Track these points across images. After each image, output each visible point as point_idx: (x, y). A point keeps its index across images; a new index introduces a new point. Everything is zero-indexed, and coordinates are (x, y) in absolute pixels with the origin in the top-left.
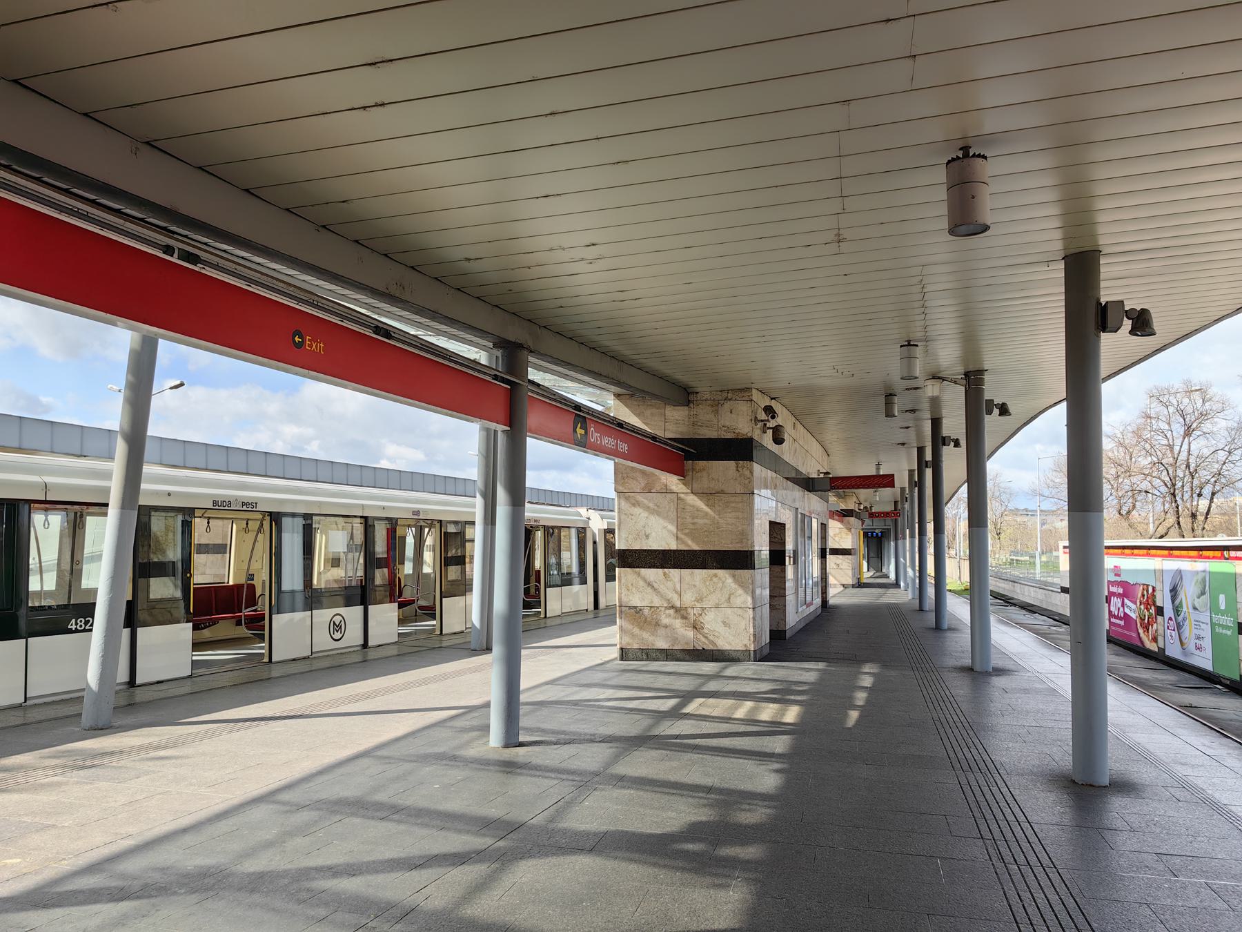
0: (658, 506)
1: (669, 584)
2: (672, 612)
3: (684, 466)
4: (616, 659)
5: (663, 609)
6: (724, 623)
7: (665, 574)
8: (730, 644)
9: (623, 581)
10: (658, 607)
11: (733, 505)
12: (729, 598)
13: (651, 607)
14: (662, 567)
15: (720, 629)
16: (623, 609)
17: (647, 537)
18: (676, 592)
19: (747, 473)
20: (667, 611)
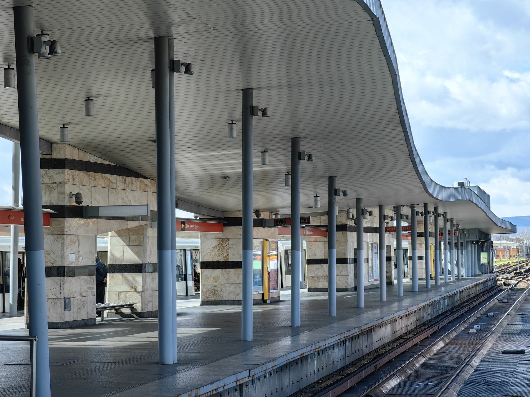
0: (319, 246)
1: (323, 269)
2: (323, 277)
3: (326, 233)
4: (306, 292)
5: (321, 276)
6: (339, 280)
7: (321, 266)
8: (341, 286)
9: (308, 268)
10: (319, 276)
11: (341, 245)
12: (341, 273)
13: (317, 276)
14: (320, 264)
16: (309, 277)
17: (316, 255)
18: (325, 271)
19: (346, 235)
20: (322, 277)
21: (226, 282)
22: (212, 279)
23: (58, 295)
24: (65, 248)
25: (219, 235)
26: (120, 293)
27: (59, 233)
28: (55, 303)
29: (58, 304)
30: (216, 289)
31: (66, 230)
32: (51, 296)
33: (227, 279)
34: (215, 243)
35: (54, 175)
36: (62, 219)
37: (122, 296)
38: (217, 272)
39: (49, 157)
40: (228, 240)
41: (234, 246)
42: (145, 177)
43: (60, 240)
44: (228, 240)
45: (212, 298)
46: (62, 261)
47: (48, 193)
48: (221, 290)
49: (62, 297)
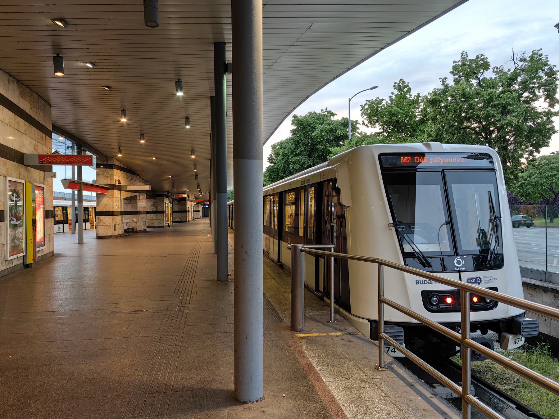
15: (183, 219)
21: (156, 219)
22: (150, 218)
23: (112, 224)
24: (114, 203)
25: (153, 200)
26: (127, 223)
27: (111, 196)
28: (110, 227)
29: (112, 227)
30: (152, 221)
31: (114, 195)
32: (108, 224)
33: (157, 218)
34: (152, 204)
35: (108, 171)
36: (112, 190)
37: (128, 224)
38: (153, 215)
39: (106, 163)
40: (157, 202)
41: (159, 205)
42: (138, 175)
43: (112, 200)
44: (157, 202)
45: (151, 225)
46: (113, 209)
47: (106, 179)
48: (154, 222)
49: (113, 224)
